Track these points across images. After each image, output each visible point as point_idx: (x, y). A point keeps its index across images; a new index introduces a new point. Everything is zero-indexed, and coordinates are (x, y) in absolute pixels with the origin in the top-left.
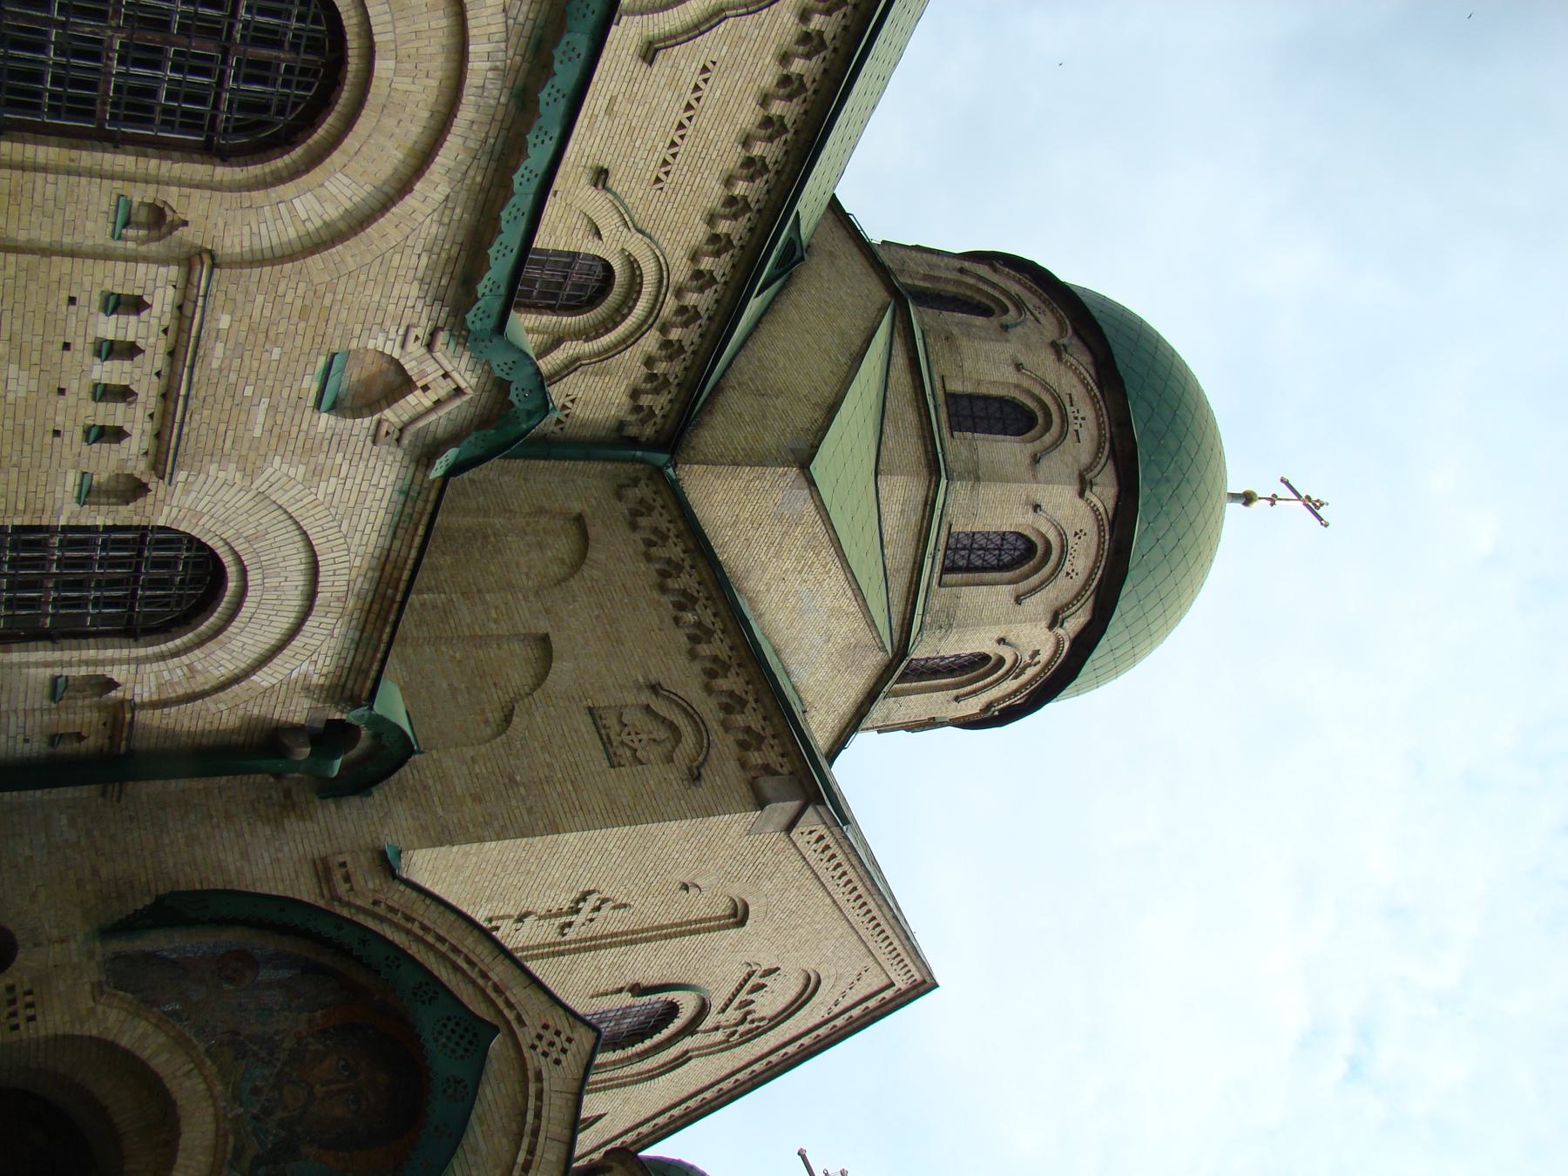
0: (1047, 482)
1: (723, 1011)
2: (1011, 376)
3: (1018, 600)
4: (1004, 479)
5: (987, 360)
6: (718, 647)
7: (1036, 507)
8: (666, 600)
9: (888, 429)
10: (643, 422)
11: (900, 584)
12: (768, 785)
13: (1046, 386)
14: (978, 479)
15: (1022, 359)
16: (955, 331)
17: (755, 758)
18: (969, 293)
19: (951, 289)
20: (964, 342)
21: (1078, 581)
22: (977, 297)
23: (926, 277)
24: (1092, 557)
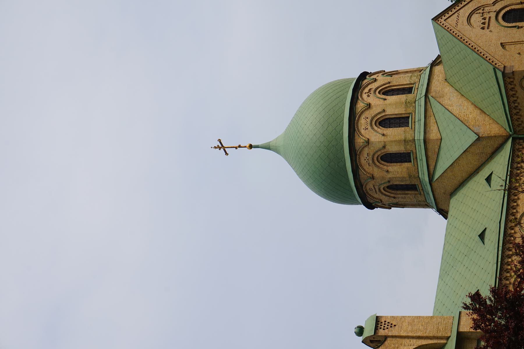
0: (381, 142)
1: (490, 18)
2: (390, 169)
3: (384, 111)
4: (395, 141)
5: (398, 172)
6: (512, 99)
7: (383, 135)
8: (519, 107)
9: (437, 150)
10: (519, 143)
11: (430, 112)
12: (511, 75)
13: (378, 167)
14: (405, 141)
15: (386, 173)
16: (408, 178)
17: (512, 80)
18: (393, 192)
19: (398, 192)
20: (405, 175)
21: (363, 116)
22: (390, 191)
23: (408, 194)
24: (359, 123)
